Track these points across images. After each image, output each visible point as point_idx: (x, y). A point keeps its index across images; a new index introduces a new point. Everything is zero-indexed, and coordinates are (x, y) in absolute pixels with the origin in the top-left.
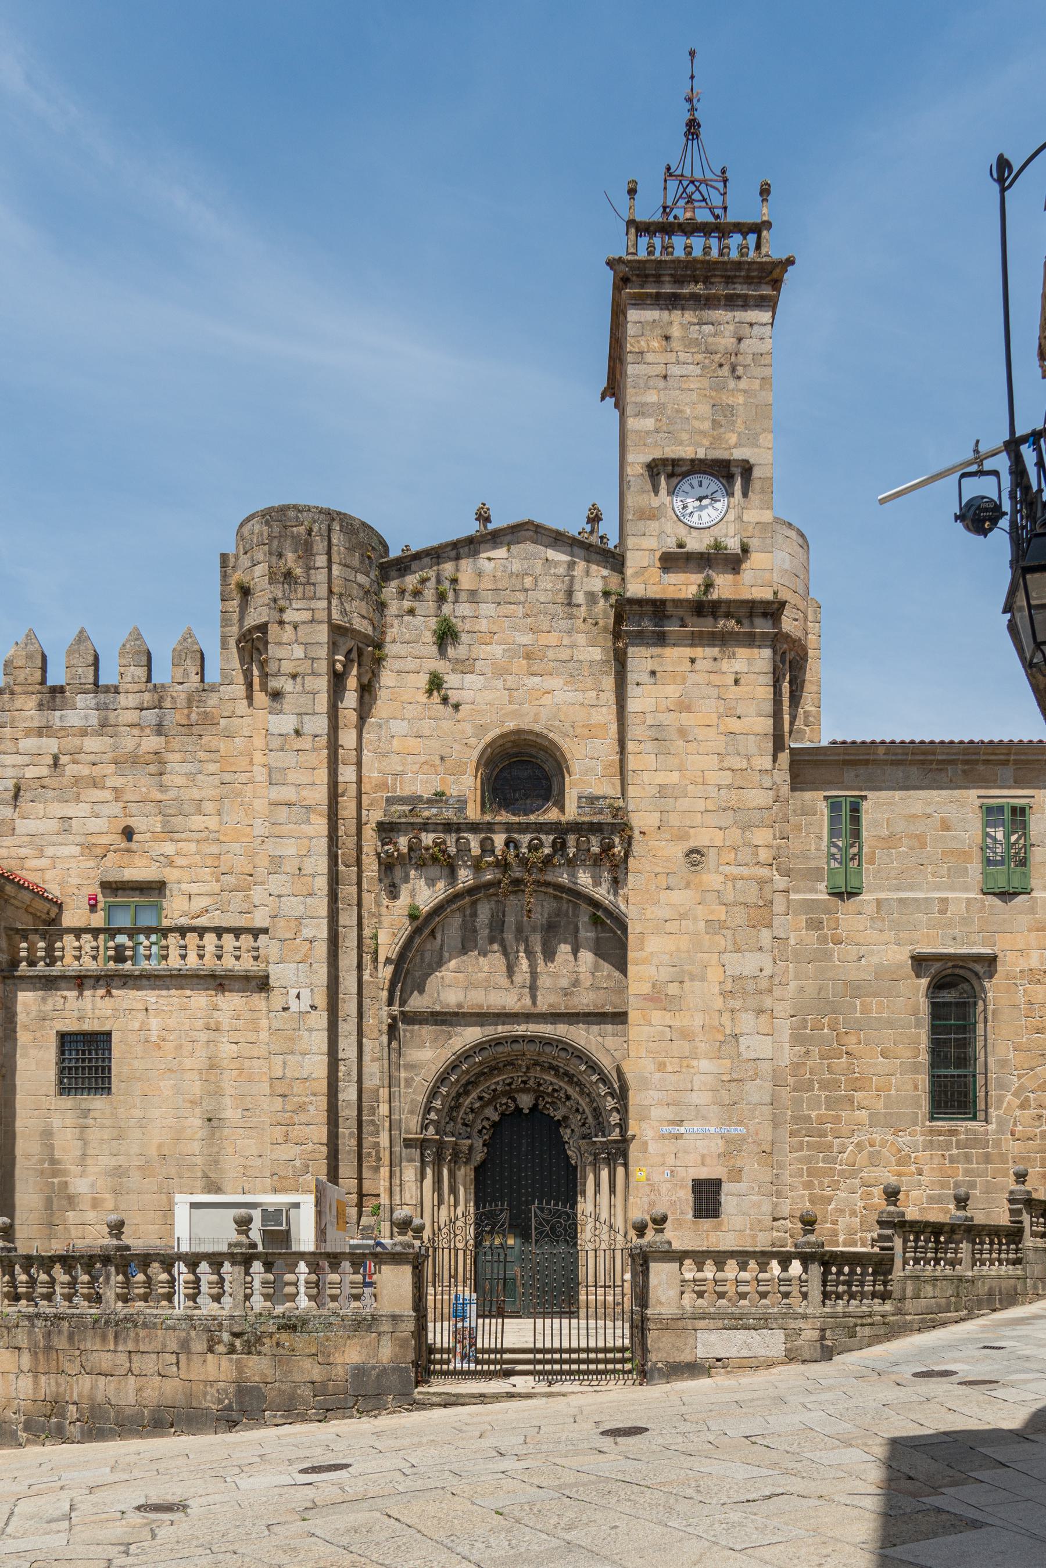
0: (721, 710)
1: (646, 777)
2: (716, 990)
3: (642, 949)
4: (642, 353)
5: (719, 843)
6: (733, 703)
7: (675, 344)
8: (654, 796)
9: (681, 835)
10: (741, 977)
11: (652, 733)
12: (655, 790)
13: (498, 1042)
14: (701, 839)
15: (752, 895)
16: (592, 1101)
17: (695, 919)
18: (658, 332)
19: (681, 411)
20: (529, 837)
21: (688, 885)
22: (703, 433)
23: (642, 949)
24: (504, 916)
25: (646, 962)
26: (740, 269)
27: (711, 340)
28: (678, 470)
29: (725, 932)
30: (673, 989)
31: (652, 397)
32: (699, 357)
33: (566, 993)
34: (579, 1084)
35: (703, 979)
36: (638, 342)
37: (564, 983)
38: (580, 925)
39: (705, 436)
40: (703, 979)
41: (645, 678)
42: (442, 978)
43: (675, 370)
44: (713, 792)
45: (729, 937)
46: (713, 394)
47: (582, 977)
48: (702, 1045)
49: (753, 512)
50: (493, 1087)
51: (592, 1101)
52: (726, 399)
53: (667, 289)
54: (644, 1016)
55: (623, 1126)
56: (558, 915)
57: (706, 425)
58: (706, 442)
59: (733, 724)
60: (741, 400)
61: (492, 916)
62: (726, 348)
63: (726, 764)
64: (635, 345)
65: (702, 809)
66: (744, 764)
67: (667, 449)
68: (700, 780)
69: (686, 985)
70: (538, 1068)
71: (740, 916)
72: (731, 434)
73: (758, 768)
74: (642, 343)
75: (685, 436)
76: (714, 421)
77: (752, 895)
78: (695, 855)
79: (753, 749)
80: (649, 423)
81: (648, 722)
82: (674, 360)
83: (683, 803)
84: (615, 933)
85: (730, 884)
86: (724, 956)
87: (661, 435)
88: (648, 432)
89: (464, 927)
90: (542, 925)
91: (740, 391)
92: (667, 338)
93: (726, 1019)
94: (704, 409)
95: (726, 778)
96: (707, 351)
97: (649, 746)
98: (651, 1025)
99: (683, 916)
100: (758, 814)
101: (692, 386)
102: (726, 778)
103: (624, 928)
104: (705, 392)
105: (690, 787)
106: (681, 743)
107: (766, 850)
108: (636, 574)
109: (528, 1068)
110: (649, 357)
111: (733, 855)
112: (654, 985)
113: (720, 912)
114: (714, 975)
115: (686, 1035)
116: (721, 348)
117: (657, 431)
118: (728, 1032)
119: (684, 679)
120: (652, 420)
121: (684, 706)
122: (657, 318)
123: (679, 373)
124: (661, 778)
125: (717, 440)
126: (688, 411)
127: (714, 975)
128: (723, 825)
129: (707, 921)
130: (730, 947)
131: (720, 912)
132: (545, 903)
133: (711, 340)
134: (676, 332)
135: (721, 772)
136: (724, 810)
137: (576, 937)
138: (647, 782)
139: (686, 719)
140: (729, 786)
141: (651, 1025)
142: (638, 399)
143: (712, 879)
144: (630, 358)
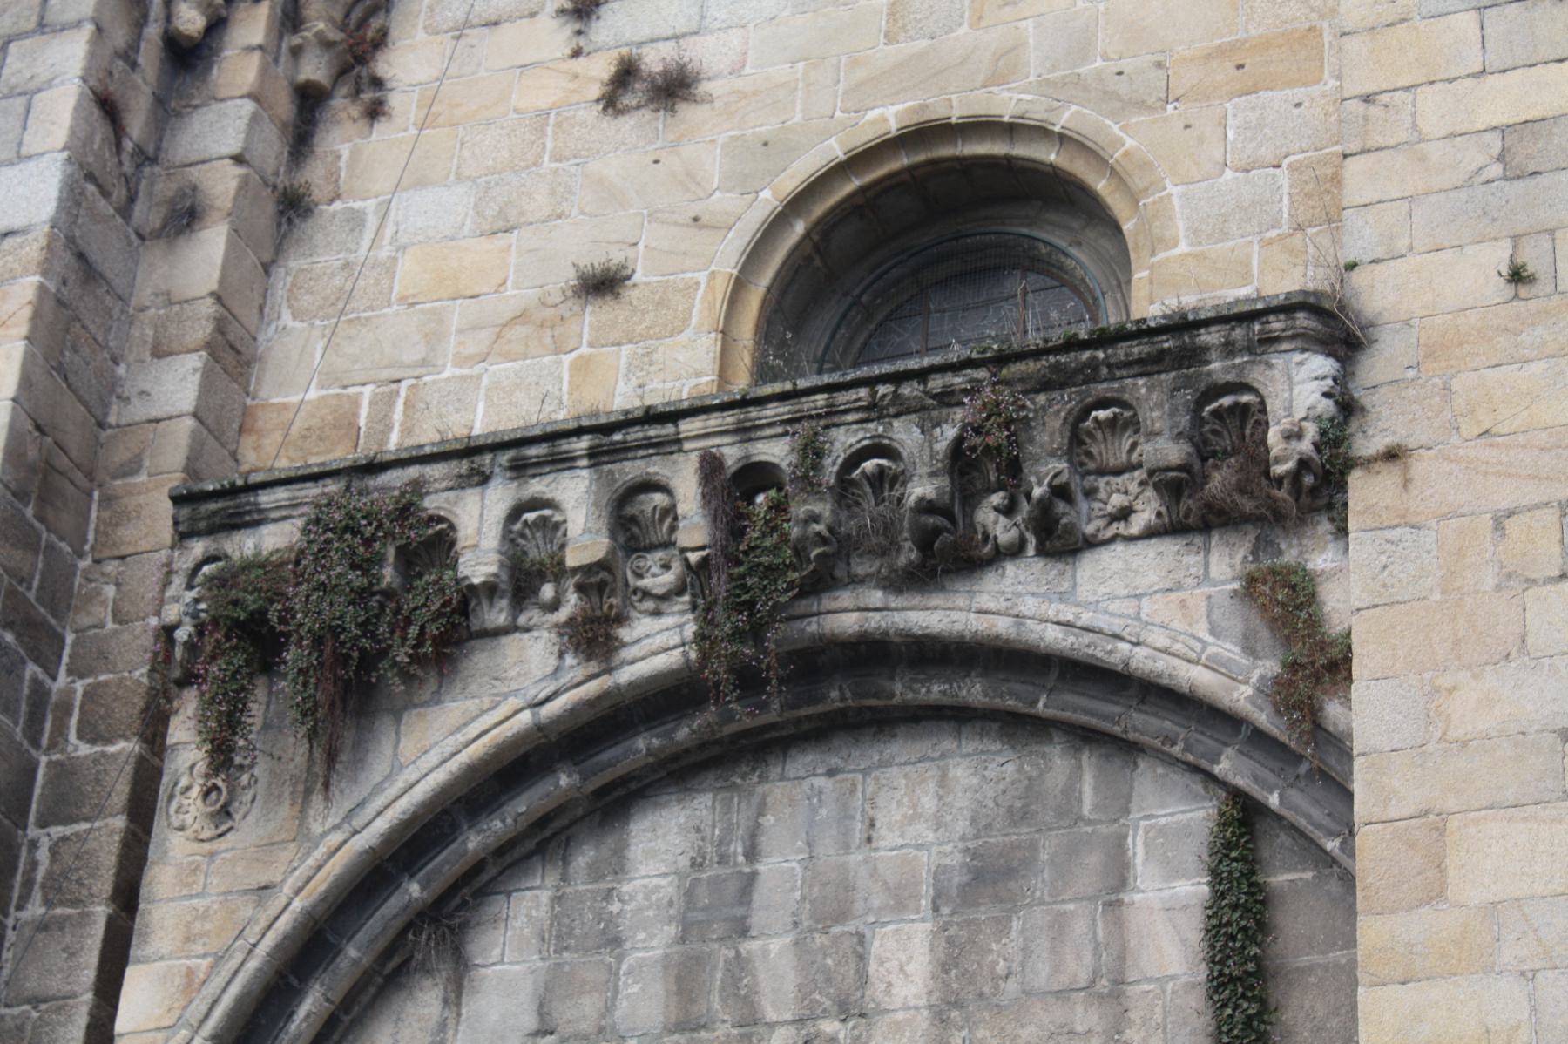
3: (1435, 894)
12: (1478, 155)
23: (1435, 894)
24: (752, 854)
38: (1137, 848)
56: (1020, 816)
61: (697, 865)
90: (939, 873)
137: (1114, 905)
138: (1432, 125)
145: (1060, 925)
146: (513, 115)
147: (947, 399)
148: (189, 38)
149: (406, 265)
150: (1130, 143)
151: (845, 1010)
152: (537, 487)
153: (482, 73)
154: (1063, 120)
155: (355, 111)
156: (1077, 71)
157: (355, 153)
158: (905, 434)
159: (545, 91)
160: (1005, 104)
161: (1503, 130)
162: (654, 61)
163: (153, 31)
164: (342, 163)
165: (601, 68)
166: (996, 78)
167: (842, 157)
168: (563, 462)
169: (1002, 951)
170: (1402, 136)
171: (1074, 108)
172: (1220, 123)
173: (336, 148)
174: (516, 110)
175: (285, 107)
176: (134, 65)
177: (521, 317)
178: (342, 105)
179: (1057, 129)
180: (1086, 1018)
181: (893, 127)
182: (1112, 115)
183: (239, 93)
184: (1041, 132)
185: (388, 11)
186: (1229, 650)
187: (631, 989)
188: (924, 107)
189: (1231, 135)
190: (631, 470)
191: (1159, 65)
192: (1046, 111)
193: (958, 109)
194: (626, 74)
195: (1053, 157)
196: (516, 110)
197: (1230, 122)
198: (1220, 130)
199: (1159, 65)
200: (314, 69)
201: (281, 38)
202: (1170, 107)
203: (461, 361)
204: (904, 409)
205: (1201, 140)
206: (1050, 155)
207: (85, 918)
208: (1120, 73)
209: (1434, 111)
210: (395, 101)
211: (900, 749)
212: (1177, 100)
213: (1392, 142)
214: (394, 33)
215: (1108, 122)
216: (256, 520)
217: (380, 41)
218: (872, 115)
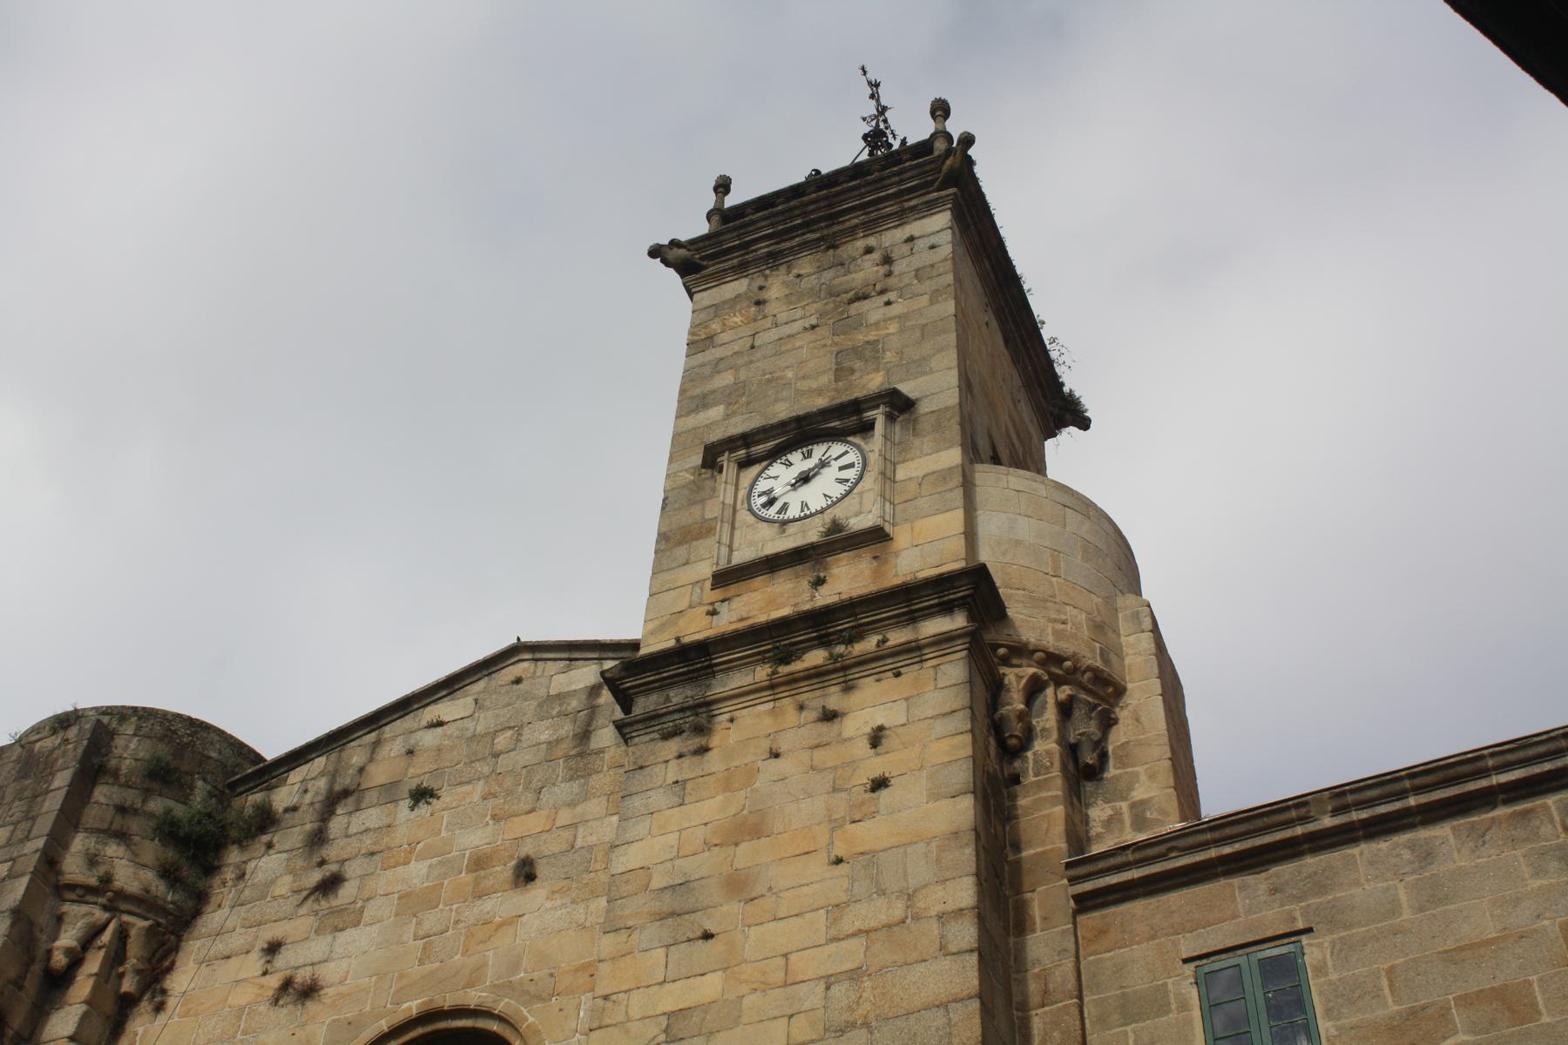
11: (667, 903)
19: (777, 379)
39: (820, 395)
44: (812, 996)
63: (850, 922)
66: (898, 910)
68: (779, 977)
79: (920, 871)
81: (658, 882)
91: (890, 319)
96: (831, 295)
102: (851, 954)
104: (823, 342)
106: (734, 908)
119: (752, 773)
121: (751, 828)
126: (790, 374)
135: (833, 947)
136: (841, 1031)
139: (745, 854)
140: (855, 975)
146: (227, 1009)
148: (57, 970)
150: (531, 1019)
153: (217, 986)
154: (500, 1008)
155: (149, 1008)
156: (511, 979)
157: (145, 1032)
159: (243, 996)
160: (474, 997)
162: (302, 976)
163: (37, 968)
164: (138, 1038)
165: (274, 981)
166: (470, 984)
167: (386, 1030)
170: (621, 1018)
171: (506, 1000)
172: (577, 1008)
173: (135, 1029)
174: (230, 1006)
175: (109, 1006)
176: (21, 987)
178: (145, 1005)
179: (496, 1012)
181: (414, 1012)
182: (525, 1005)
183: (79, 1001)
184: (488, 1014)
185: (177, 952)
188: (431, 1001)
189: (582, 1014)
191: (552, 975)
192: (493, 1002)
193: (448, 1002)
194: (287, 984)
195: (495, 1028)
196: (230, 1006)
197: (582, 1007)
198: (577, 1011)
199: (552, 975)
200: (128, 985)
201: (112, 967)
202: (554, 999)
205: (566, 1018)
206: (494, 1027)
208: (532, 980)
210: (171, 1002)
212: (558, 995)
213: (614, 1022)
214: (178, 963)
215: (522, 1008)
217: (170, 969)
218: (405, 1005)
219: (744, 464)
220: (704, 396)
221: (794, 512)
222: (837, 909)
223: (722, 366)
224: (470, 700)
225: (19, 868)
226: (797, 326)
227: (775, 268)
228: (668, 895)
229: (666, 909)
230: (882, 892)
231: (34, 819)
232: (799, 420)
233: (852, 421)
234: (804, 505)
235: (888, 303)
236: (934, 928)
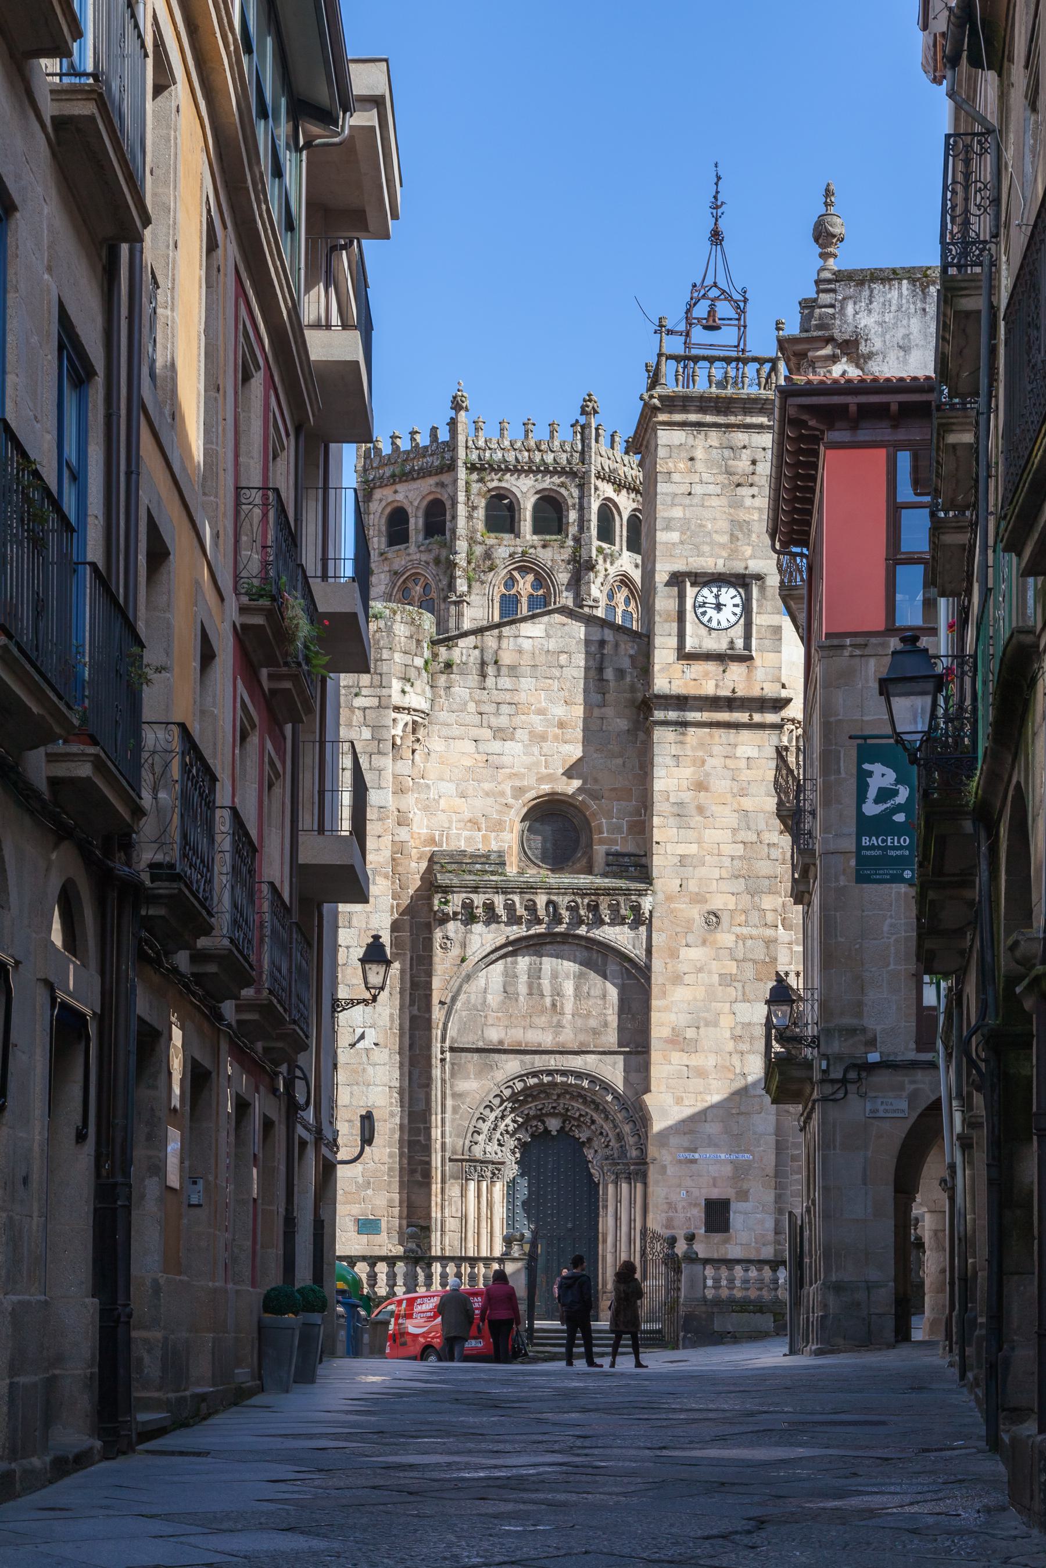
0: (735, 791)
1: (670, 848)
2: (728, 1034)
4: (669, 473)
5: (732, 907)
6: (745, 785)
7: (699, 466)
8: (675, 865)
9: (698, 899)
10: (749, 1024)
11: (675, 810)
12: (676, 860)
13: (534, 1074)
14: (718, 902)
15: (760, 954)
16: (615, 1127)
17: (710, 972)
18: (685, 455)
19: (704, 526)
20: (567, 898)
21: (704, 942)
22: (723, 546)
25: (667, 1009)
26: (757, 404)
27: (731, 462)
28: (700, 580)
29: (736, 984)
30: (690, 1033)
31: (677, 513)
32: (722, 478)
33: (595, 1032)
34: (604, 1111)
35: (716, 1024)
36: (667, 463)
37: (593, 1023)
38: (608, 972)
40: (716, 1024)
41: (669, 761)
42: (486, 1017)
43: (698, 489)
44: (727, 862)
45: (740, 988)
46: (732, 511)
47: (609, 1018)
48: (715, 1082)
49: (764, 617)
50: (526, 1112)
51: (615, 1127)
52: (743, 515)
53: (693, 417)
54: (664, 1057)
55: (643, 1150)
57: (724, 539)
58: (725, 554)
59: (747, 803)
60: (756, 517)
62: (744, 470)
64: (665, 466)
65: (718, 877)
66: (753, 838)
67: (690, 560)
68: (716, 852)
69: (702, 1030)
70: (568, 1097)
71: (749, 971)
72: (746, 547)
73: (767, 842)
74: (670, 464)
75: (706, 548)
76: (732, 535)
77: (760, 954)
78: (713, 919)
79: (762, 826)
80: (674, 536)
81: (672, 800)
82: (697, 480)
83: (702, 872)
84: (638, 980)
85: (741, 942)
86: (734, 1005)
87: (686, 546)
88: (673, 544)
89: (506, 974)
90: (574, 972)
91: (755, 508)
92: (692, 459)
93: (736, 1060)
94: (724, 525)
95: (739, 850)
97: (672, 821)
98: (670, 1064)
99: (700, 970)
100: (767, 882)
101: (714, 504)
102: (739, 850)
103: (648, 979)
105: (708, 857)
106: (698, 818)
107: (772, 913)
108: (662, 670)
109: (559, 1096)
110: (676, 477)
111: (743, 918)
112: (673, 1029)
113: (732, 967)
114: (726, 1021)
115: (701, 1073)
116: (740, 471)
117: (682, 542)
118: (738, 1071)
119: (703, 762)
120: (678, 534)
122: (683, 442)
123: (702, 492)
124: (682, 849)
125: (734, 554)
126: (710, 526)
127: (726, 1021)
128: (735, 891)
129: (720, 975)
130: (740, 998)
131: (732, 967)
132: (577, 953)
133: (731, 462)
134: (699, 454)
141: (670, 1064)
142: (666, 515)
143: (726, 938)
144: (659, 479)
145: (595, 984)
147: (587, 894)
149: (442, 802)
151: (558, 995)
152: (509, 896)
158: (579, 900)
161: (681, 856)
168: (515, 893)
169: (585, 989)
177: (470, 821)
180: (600, 1002)
186: (630, 947)
187: (520, 986)
190: (527, 897)
203: (457, 829)
204: (578, 894)
207: (405, 954)
209: (669, 847)
211: (566, 947)
216: (453, 892)
219: (693, 585)
220: (670, 520)
221: (714, 624)
222: (735, 831)
223: (677, 500)
224: (542, 627)
225: (383, 702)
226: (712, 489)
227: (699, 433)
228: (676, 806)
229: (676, 812)
230: (749, 829)
231: (381, 675)
232: (720, 574)
233: (740, 582)
234: (719, 623)
235: (753, 496)
236: (766, 848)
